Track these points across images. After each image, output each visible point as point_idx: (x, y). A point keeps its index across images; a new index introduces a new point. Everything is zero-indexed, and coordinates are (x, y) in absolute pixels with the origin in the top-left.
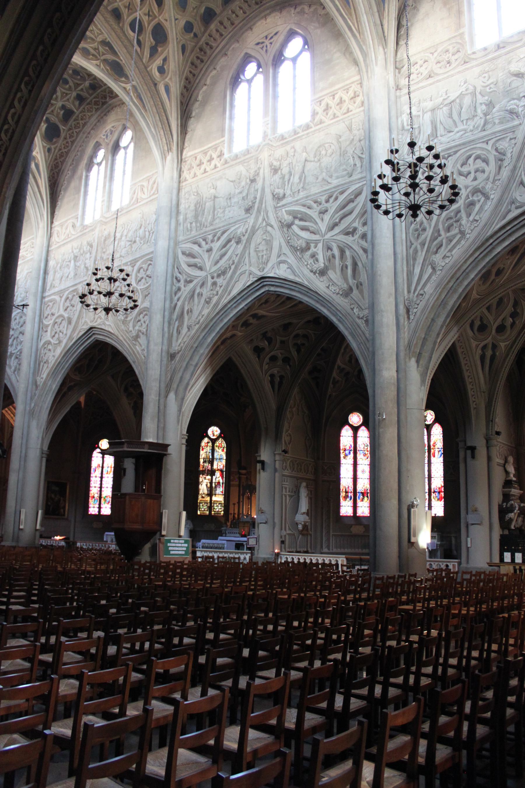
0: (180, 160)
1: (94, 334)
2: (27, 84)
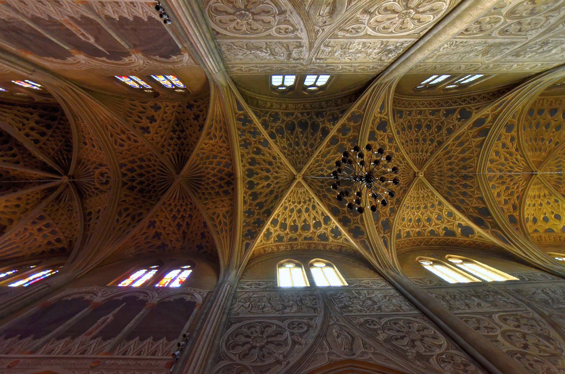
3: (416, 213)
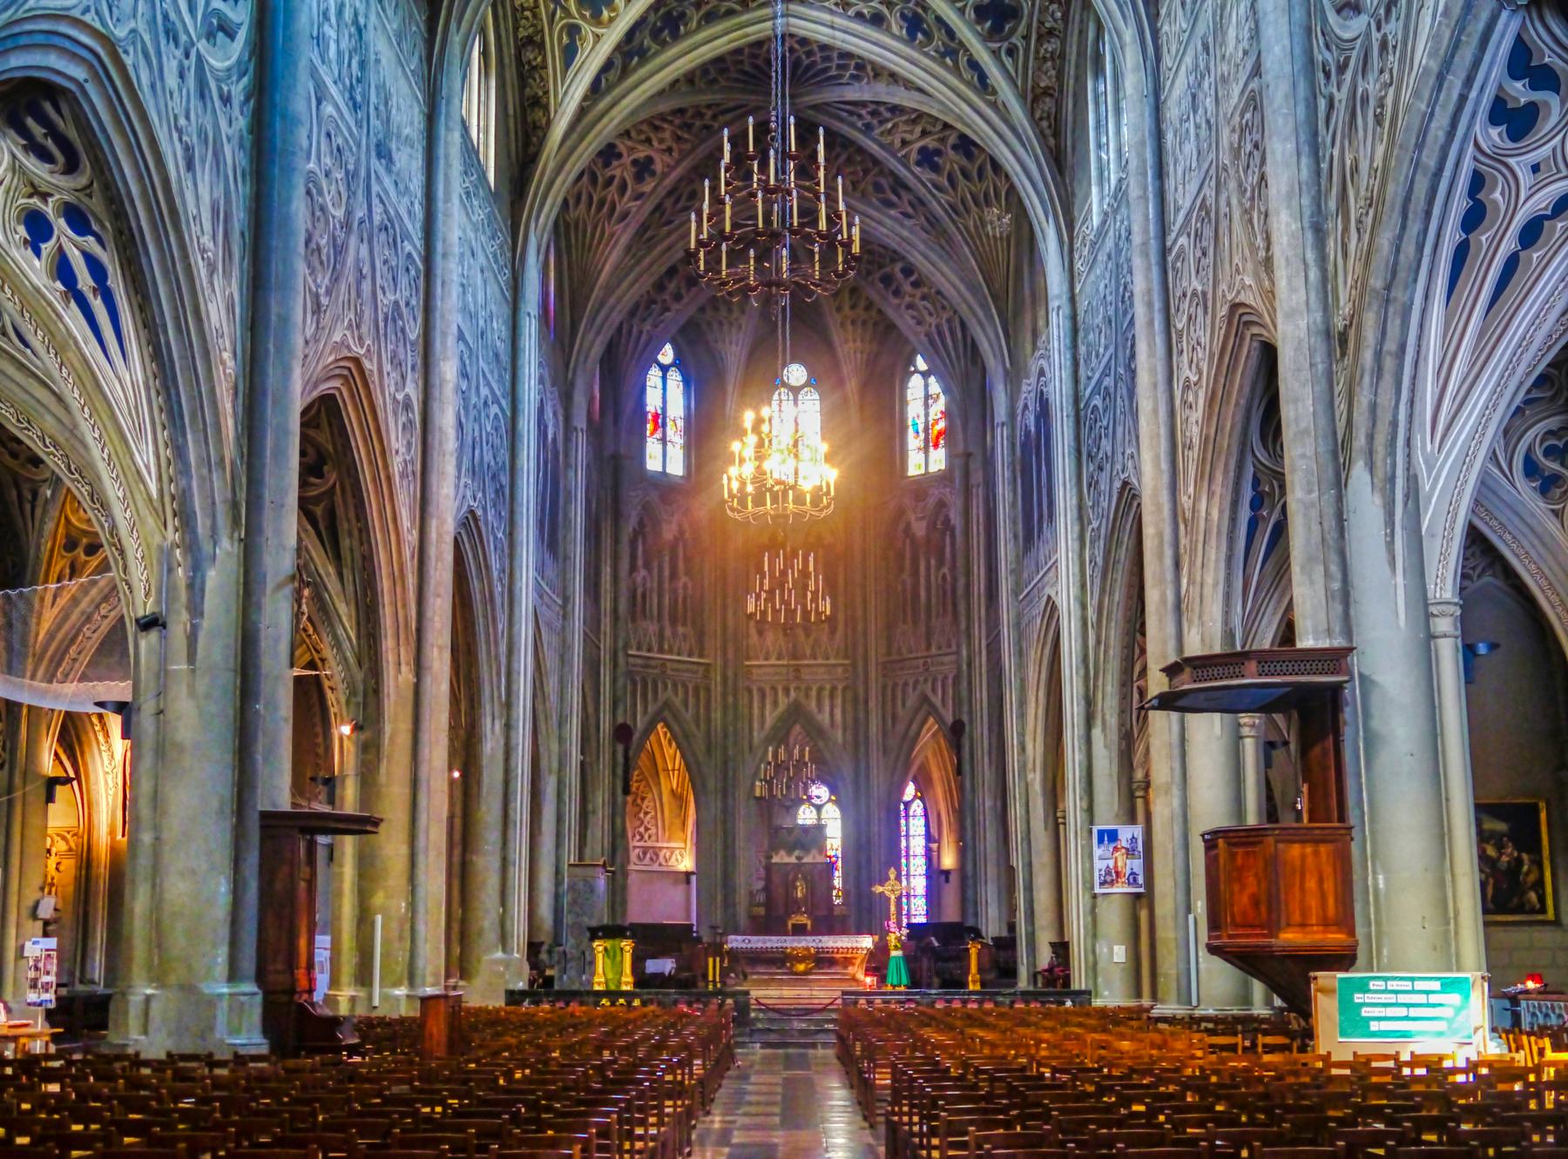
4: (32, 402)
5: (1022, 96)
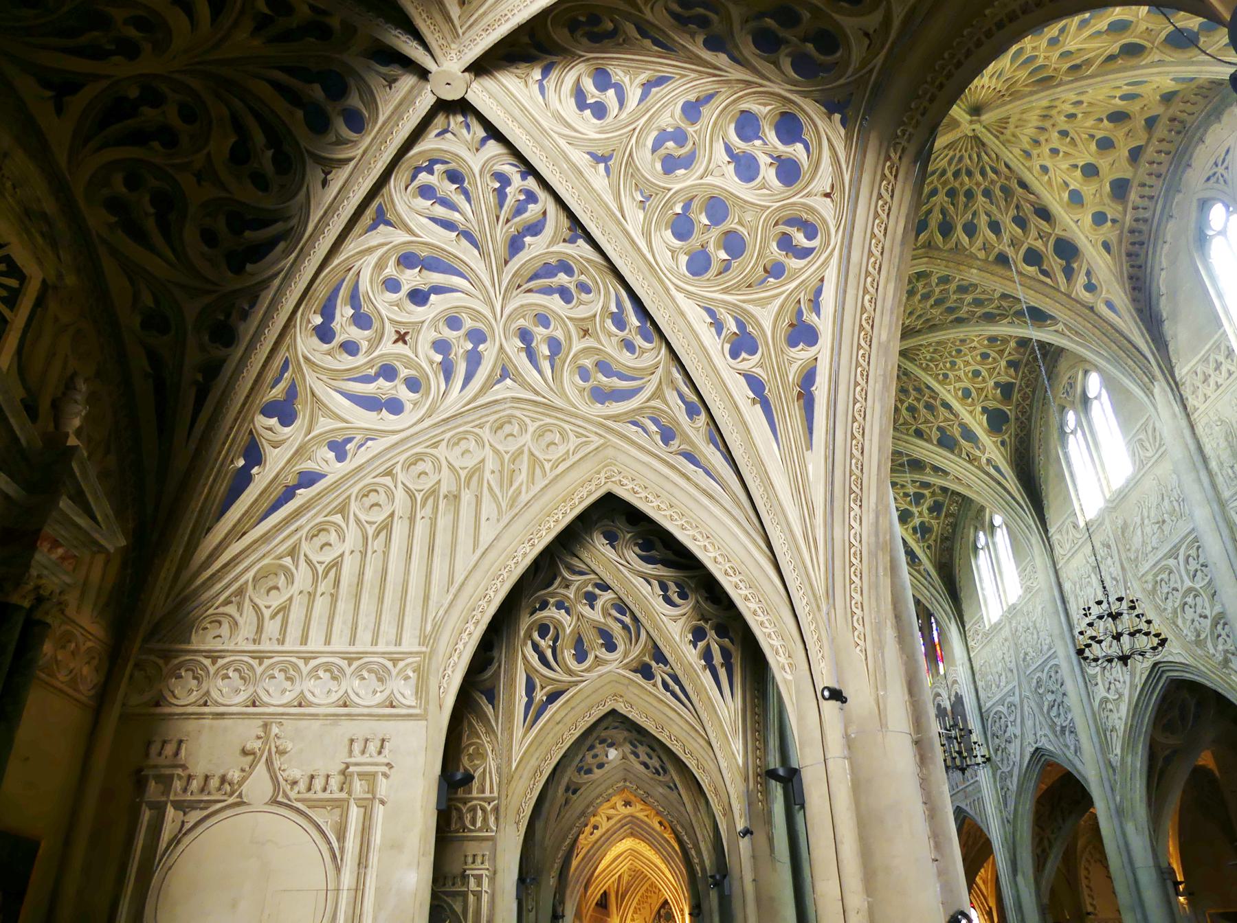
0: (1175, 386)
1: (1163, 671)
2: (855, 501)
3: (973, 345)
4: (665, 718)
5: (935, 567)
